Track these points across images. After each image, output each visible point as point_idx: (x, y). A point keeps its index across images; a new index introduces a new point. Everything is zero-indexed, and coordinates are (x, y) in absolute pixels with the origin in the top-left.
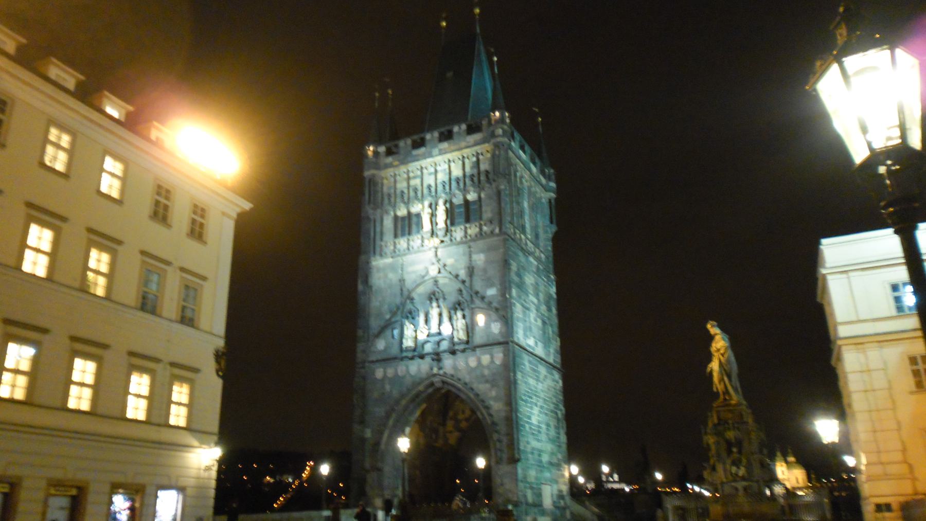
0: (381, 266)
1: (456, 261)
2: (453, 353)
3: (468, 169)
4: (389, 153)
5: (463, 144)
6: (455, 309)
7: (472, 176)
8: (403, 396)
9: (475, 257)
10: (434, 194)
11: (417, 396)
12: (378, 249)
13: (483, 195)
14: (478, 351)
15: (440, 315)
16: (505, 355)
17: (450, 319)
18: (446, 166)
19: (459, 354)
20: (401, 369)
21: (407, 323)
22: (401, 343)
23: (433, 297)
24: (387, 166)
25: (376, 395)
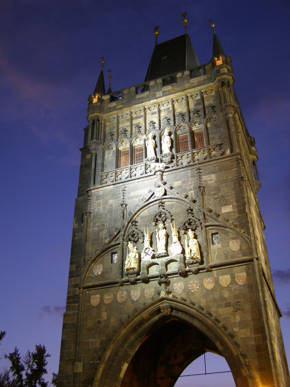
0: (101, 193)
1: (183, 182)
2: (184, 274)
3: (192, 106)
4: (113, 99)
5: (187, 85)
6: (186, 229)
7: (197, 111)
8: (122, 324)
9: (204, 178)
10: (157, 128)
11: (140, 324)
12: (98, 179)
13: (209, 126)
14: (215, 272)
15: (168, 236)
16: (248, 274)
17: (179, 239)
18: (170, 106)
19: (191, 276)
20: (121, 294)
21: (130, 245)
22: (123, 264)
23: (157, 219)
24: (110, 110)
25: (89, 324)
